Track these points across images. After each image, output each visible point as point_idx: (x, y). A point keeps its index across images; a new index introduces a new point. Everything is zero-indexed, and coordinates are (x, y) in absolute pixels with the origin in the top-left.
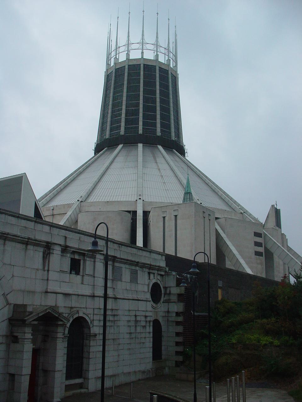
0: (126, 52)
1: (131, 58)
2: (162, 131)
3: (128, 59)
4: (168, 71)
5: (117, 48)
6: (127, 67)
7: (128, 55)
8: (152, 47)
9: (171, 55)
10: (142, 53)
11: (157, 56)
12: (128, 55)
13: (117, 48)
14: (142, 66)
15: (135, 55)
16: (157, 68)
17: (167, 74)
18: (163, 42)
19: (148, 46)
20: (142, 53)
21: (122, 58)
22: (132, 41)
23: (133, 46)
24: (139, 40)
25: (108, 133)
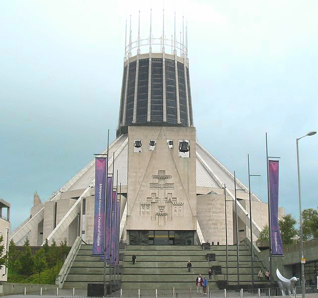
0: (137, 48)
1: (142, 53)
2: (168, 117)
3: (139, 55)
4: (174, 61)
5: (131, 44)
6: (138, 62)
7: (139, 50)
8: (160, 40)
9: (179, 45)
10: (151, 48)
11: (164, 48)
12: (139, 50)
13: (131, 44)
14: (150, 60)
15: (144, 51)
16: (164, 60)
17: (174, 65)
18: (168, 36)
19: (156, 41)
20: (151, 48)
21: (134, 54)
22: (142, 38)
23: (143, 43)
24: (147, 36)
25: (124, 121)
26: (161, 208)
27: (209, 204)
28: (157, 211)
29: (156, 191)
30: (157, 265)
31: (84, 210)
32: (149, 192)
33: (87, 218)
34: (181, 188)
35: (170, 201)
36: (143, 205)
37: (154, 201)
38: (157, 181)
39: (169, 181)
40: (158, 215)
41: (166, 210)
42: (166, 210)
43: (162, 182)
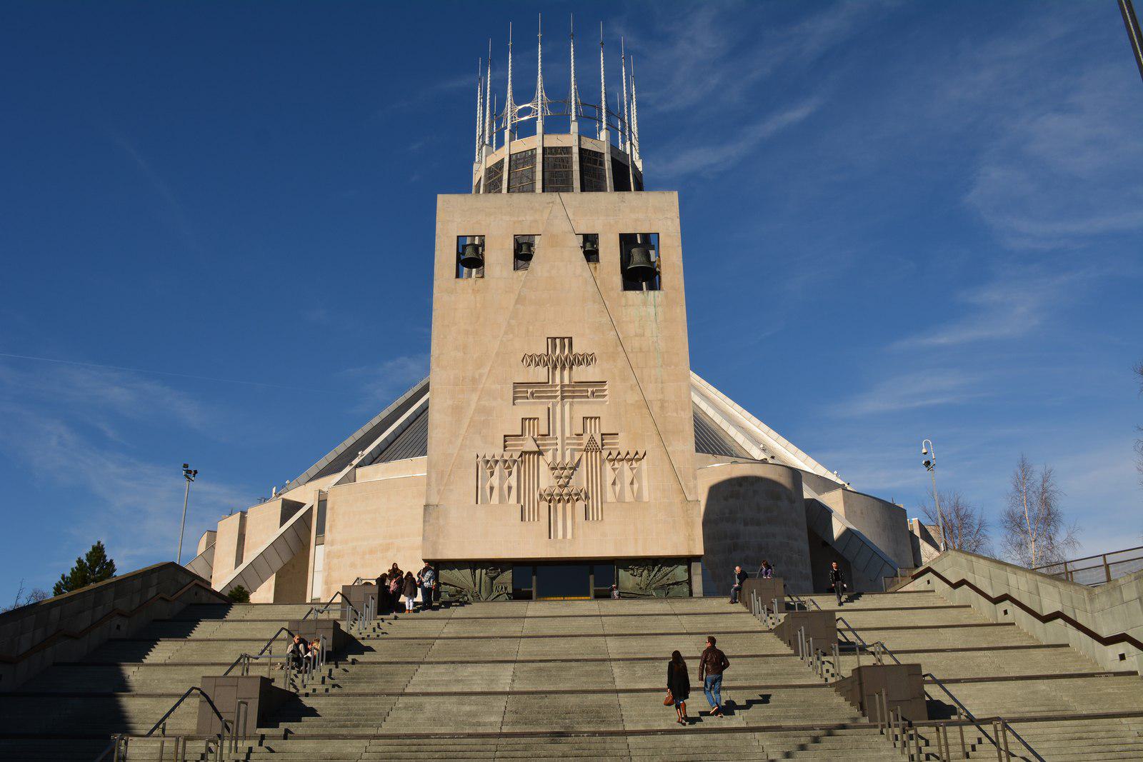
6: (506, 160)
14: (540, 151)
26: (557, 472)
27: (726, 499)
28: (547, 481)
29: (537, 409)
30: (504, 678)
31: (321, 530)
32: (510, 418)
33: (328, 555)
34: (633, 398)
35: (592, 448)
36: (490, 463)
37: (530, 446)
38: (540, 374)
39: (582, 373)
40: (551, 498)
41: (580, 481)
42: (580, 481)
43: (562, 377)
